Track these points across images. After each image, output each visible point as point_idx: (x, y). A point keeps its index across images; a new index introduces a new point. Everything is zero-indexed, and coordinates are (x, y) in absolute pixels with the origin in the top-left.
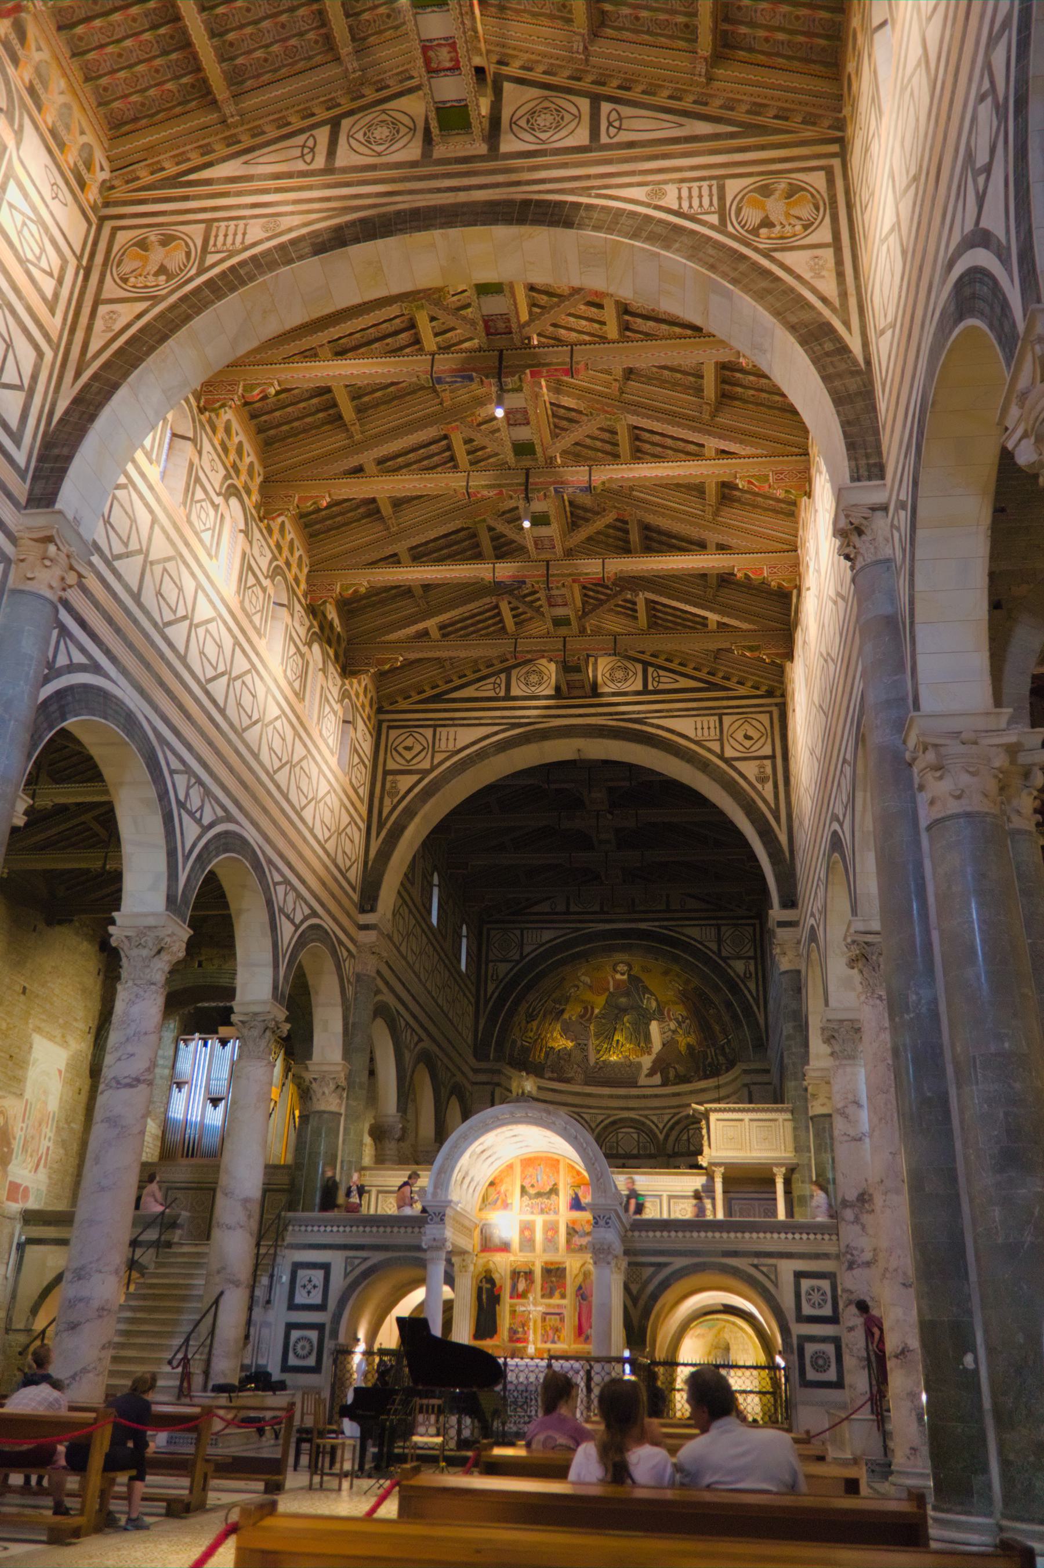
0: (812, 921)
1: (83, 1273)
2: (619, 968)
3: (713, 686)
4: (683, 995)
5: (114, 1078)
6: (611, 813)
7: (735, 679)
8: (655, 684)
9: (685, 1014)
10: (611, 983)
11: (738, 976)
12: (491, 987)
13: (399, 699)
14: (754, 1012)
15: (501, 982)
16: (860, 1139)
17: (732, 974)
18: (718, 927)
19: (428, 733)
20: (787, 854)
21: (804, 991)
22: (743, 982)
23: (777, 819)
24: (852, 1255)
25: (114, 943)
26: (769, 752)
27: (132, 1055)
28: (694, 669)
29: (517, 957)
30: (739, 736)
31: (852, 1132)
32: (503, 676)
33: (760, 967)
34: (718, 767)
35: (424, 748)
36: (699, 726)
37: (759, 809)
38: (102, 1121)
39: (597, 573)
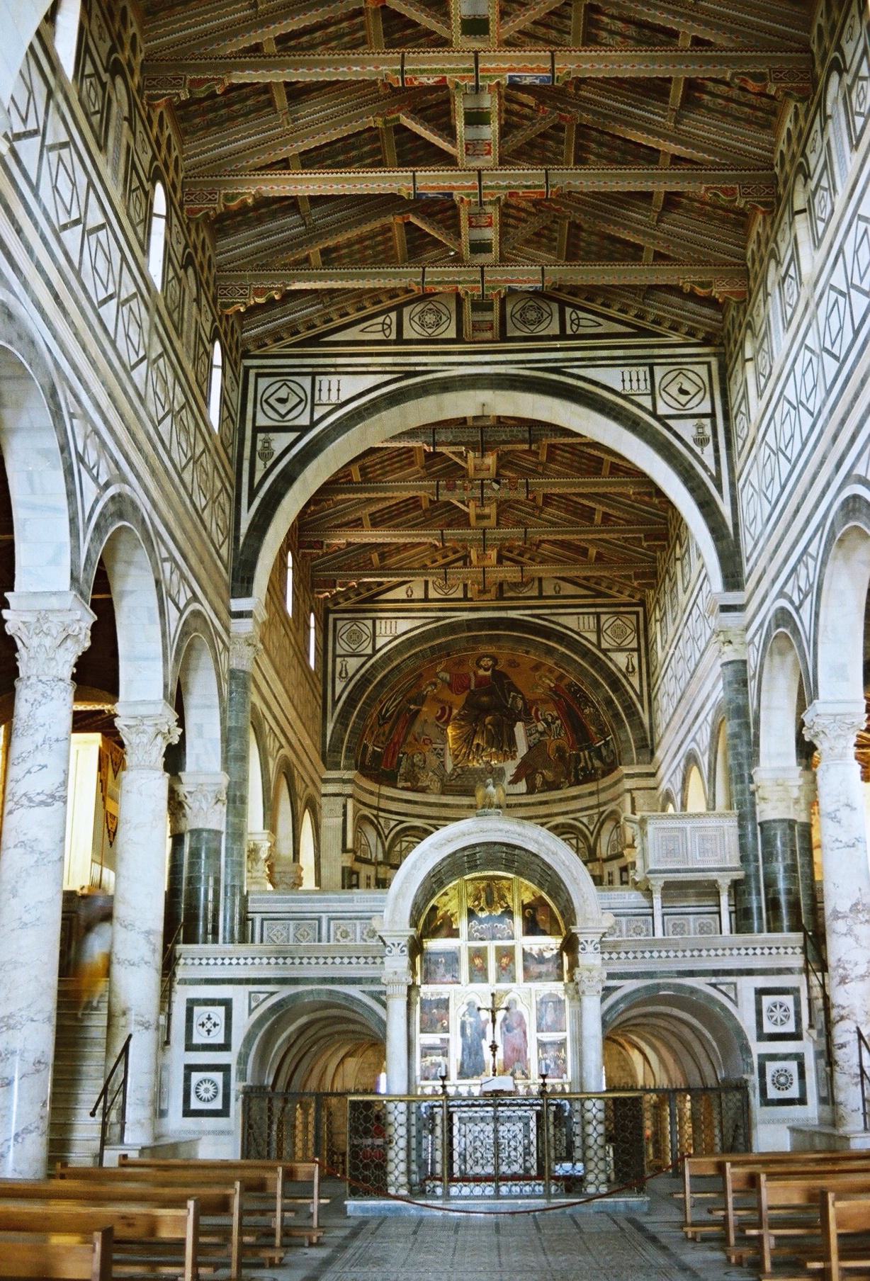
0: (783, 603)
1: (11, 1022)
2: (482, 663)
3: (643, 332)
4: (555, 692)
5: (25, 795)
6: (498, 482)
7: (667, 324)
8: (575, 327)
9: (555, 714)
11: (620, 670)
12: (339, 686)
13: (268, 341)
15: (350, 680)
16: (853, 845)
17: (613, 668)
18: (598, 615)
19: (306, 382)
20: (731, 529)
21: (752, 685)
22: (625, 677)
23: (719, 487)
24: (844, 969)
25: (10, 629)
26: (709, 411)
27: (45, 766)
28: (620, 310)
29: (369, 651)
30: (673, 390)
31: (844, 839)
32: (393, 315)
33: (644, 660)
34: (651, 426)
35: (301, 401)
36: (627, 378)
37: (698, 476)
38: (15, 846)
39: (540, 186)
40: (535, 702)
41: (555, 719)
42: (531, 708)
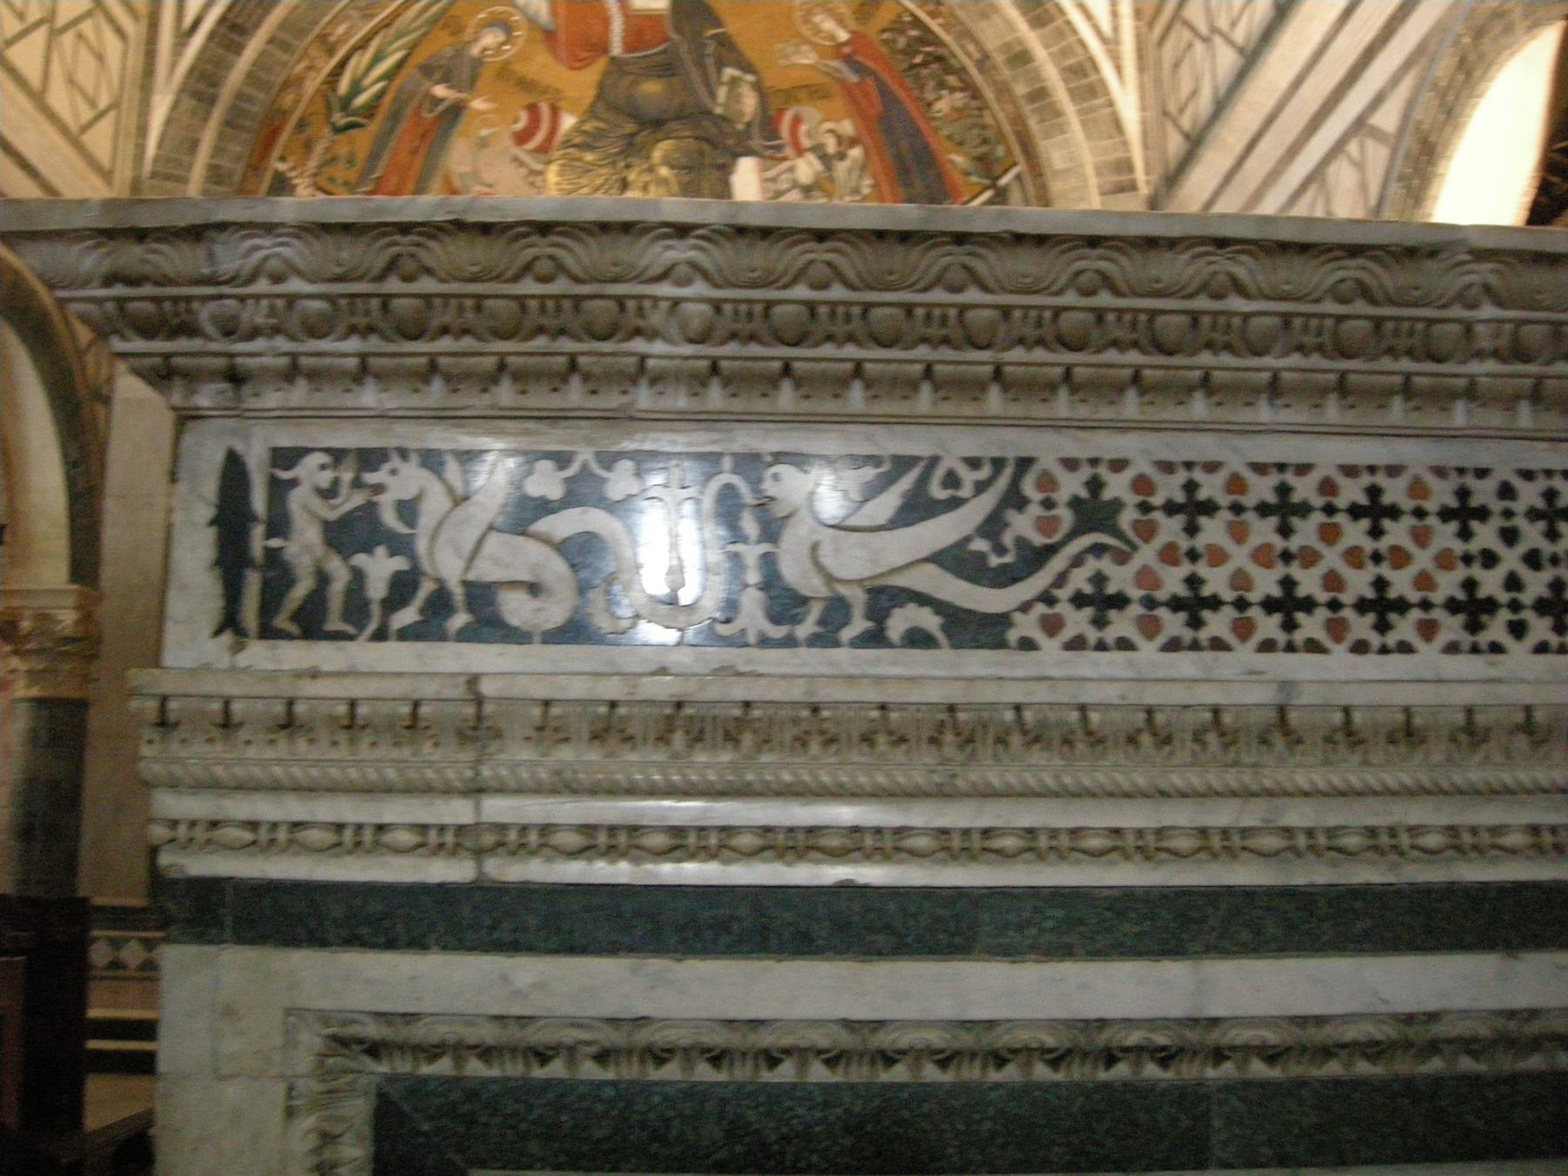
4: (848, 60)
9: (847, 127)
10: (617, 27)
14: (1102, 82)
40: (790, 95)
41: (846, 142)
42: (781, 111)
